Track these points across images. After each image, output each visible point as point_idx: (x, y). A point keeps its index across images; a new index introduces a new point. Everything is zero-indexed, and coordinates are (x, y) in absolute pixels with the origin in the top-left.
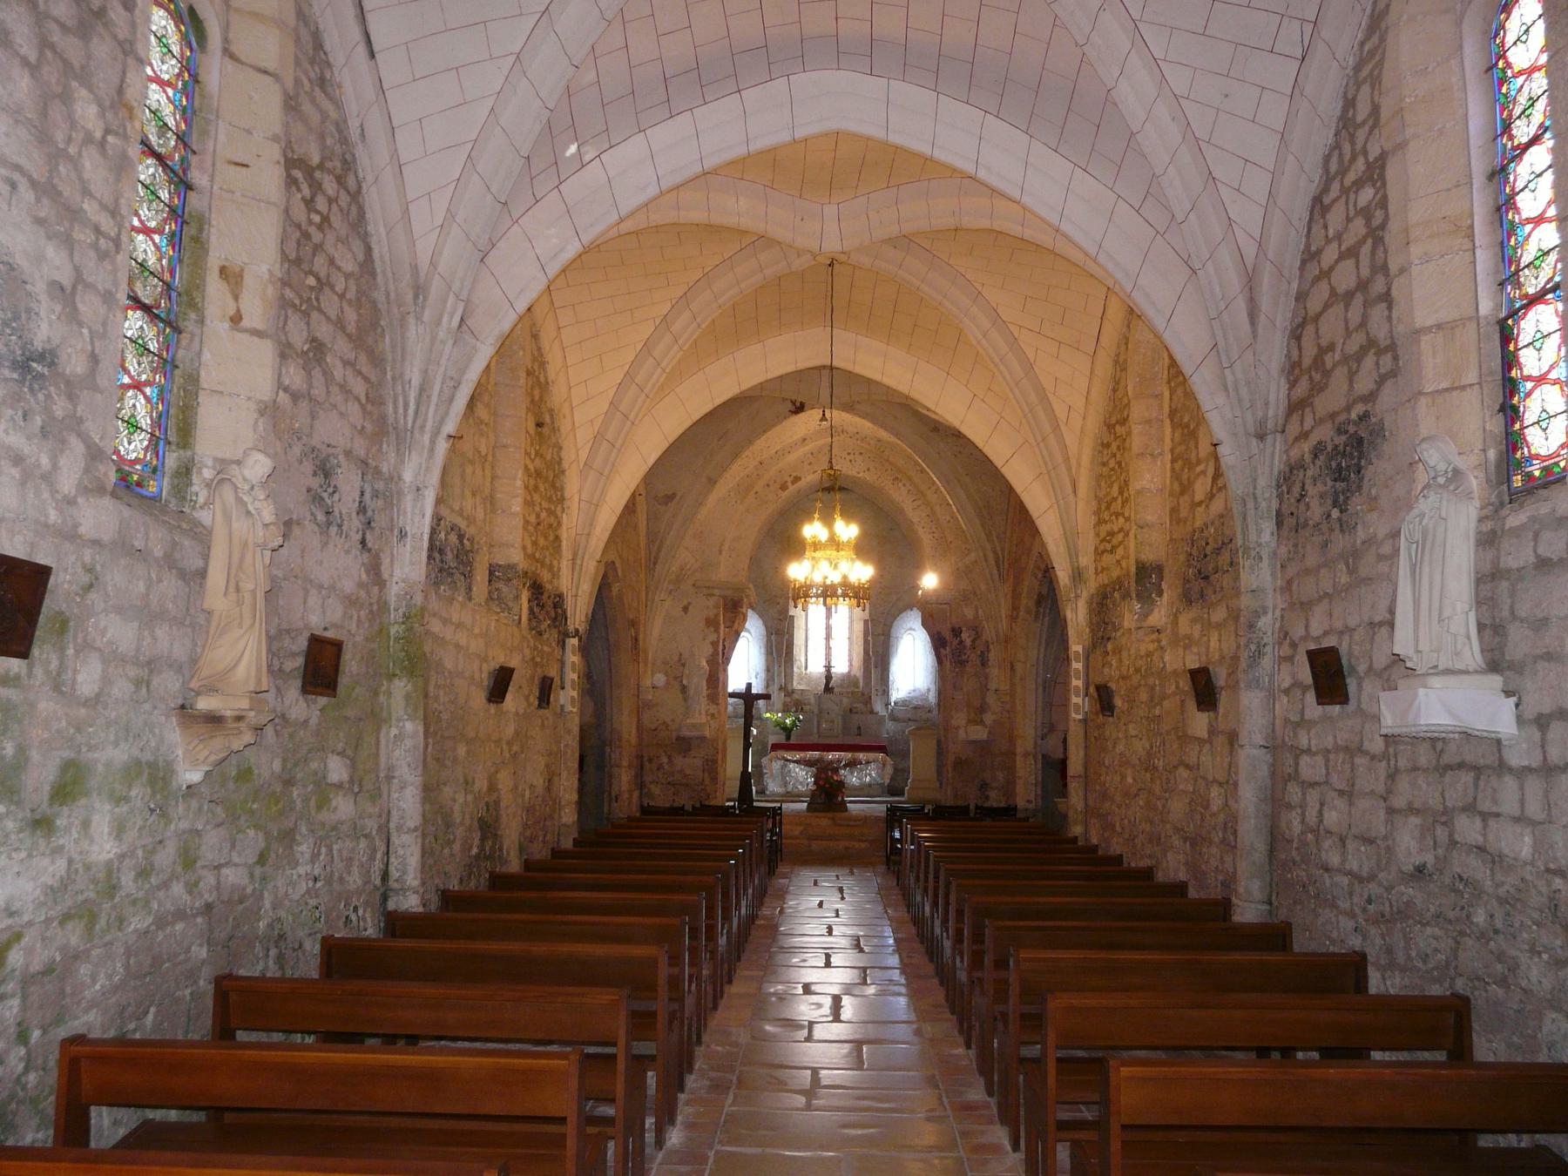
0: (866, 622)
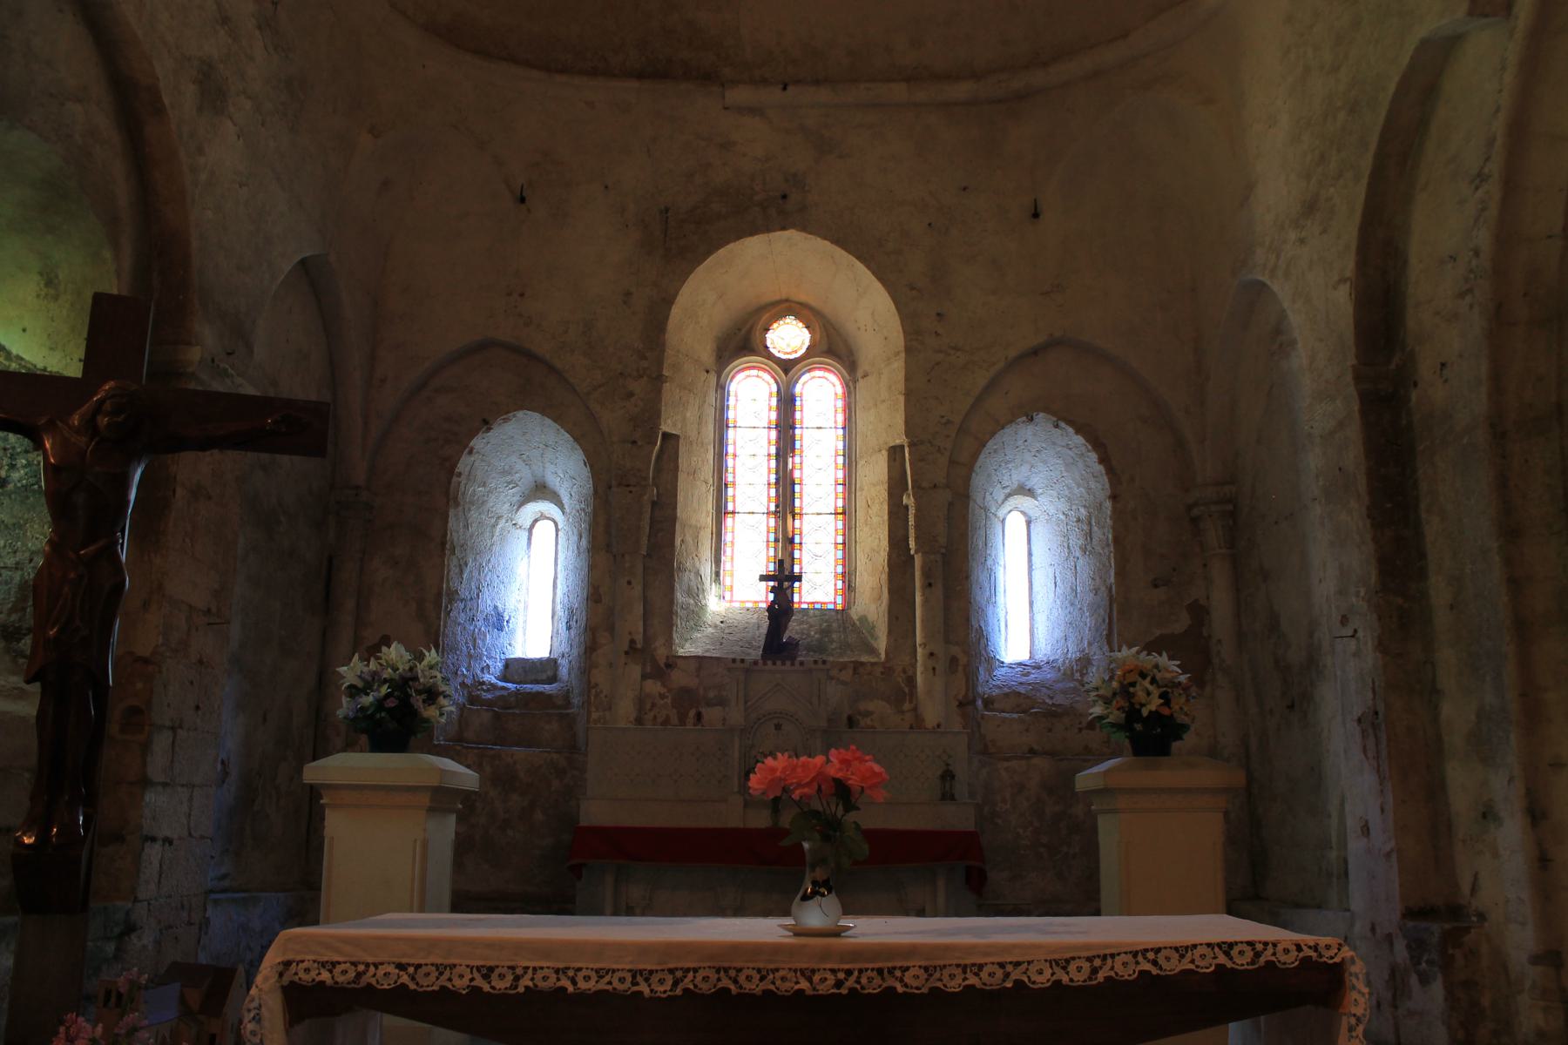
0: (895, 453)
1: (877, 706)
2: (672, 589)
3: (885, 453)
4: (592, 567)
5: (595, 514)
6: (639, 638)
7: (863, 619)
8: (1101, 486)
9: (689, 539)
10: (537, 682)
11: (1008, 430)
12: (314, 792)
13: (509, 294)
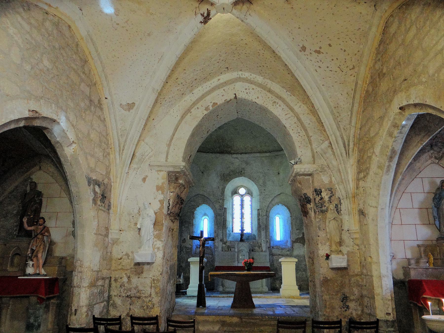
1: (257, 248)
2: (226, 231)
7: (254, 235)
12: (189, 262)
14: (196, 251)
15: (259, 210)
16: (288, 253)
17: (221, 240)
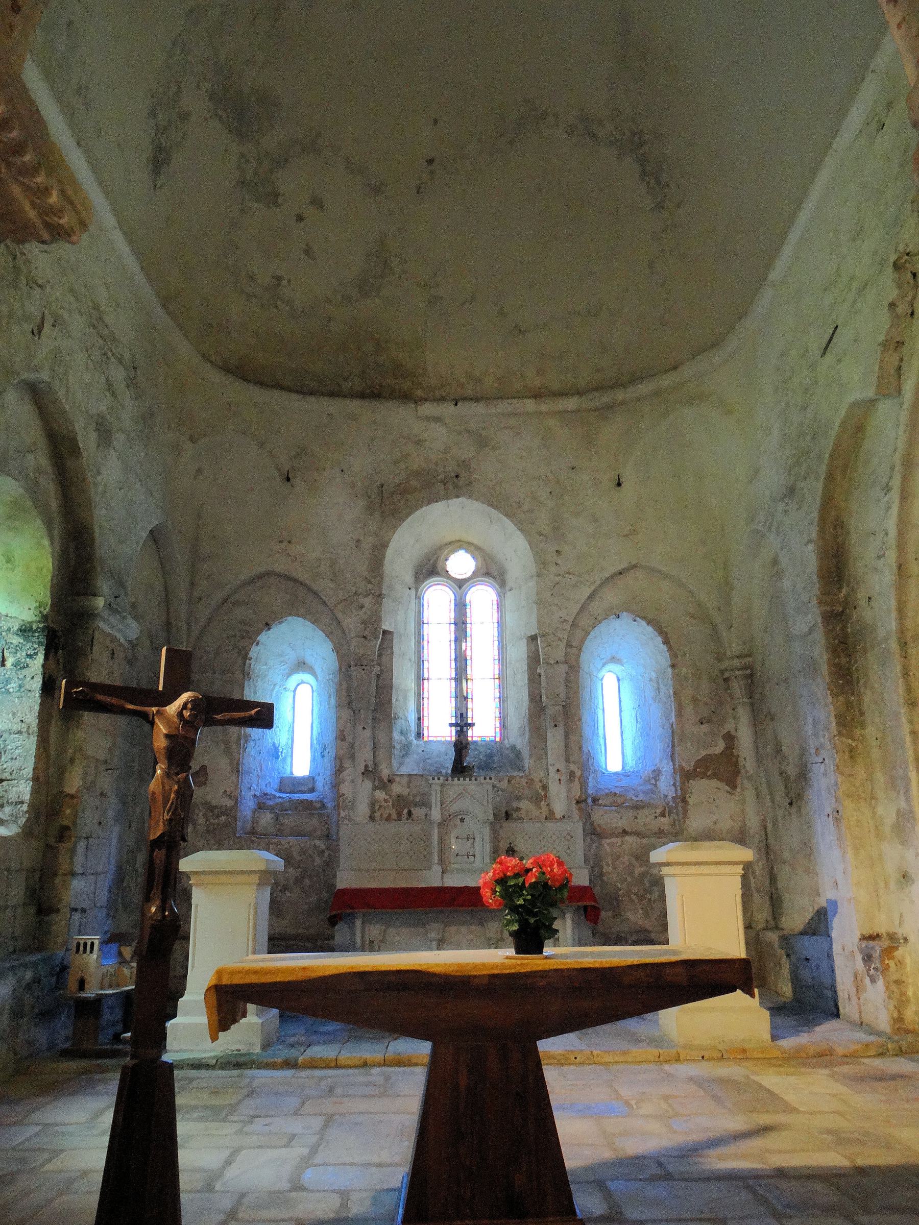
1: (525, 805)
3: (525, 641)
4: (338, 718)
5: (340, 684)
6: (371, 764)
7: (513, 748)
8: (664, 658)
9: (401, 698)
10: (302, 792)
11: (605, 623)
13: (281, 542)
14: (255, 822)
15: (533, 638)
16: (665, 822)
17: (367, 772)
